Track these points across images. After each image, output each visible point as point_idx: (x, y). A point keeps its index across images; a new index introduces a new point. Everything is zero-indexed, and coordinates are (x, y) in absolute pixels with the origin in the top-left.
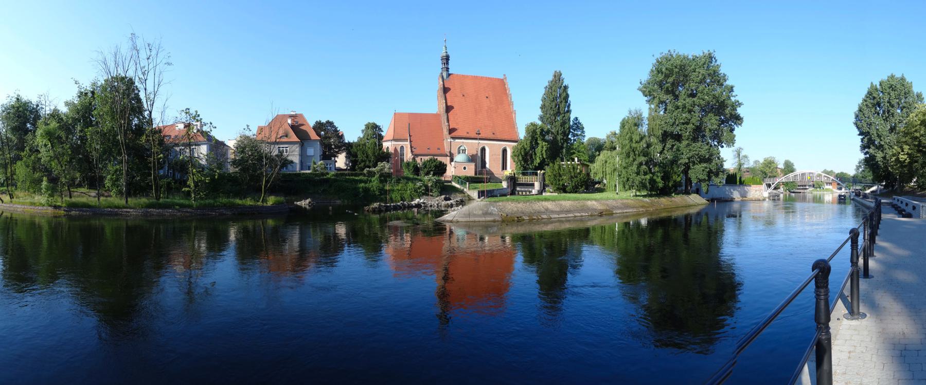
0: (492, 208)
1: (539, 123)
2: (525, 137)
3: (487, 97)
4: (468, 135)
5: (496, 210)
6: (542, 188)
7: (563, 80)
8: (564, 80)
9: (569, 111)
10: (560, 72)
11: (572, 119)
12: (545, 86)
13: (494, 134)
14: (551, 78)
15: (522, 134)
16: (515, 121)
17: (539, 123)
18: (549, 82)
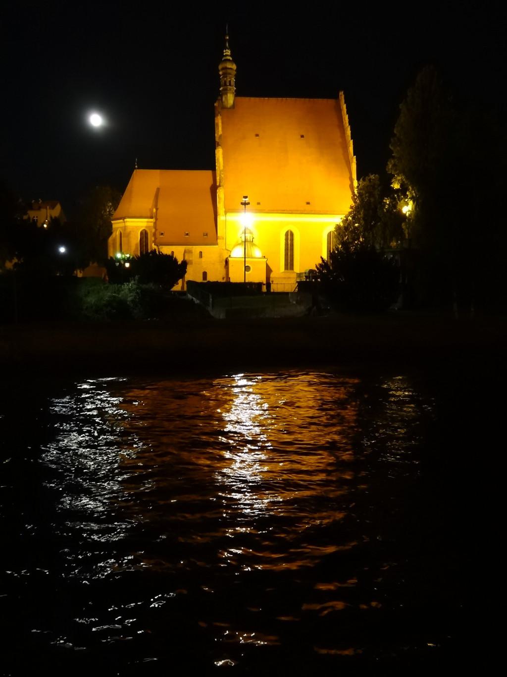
13: (308, 203)
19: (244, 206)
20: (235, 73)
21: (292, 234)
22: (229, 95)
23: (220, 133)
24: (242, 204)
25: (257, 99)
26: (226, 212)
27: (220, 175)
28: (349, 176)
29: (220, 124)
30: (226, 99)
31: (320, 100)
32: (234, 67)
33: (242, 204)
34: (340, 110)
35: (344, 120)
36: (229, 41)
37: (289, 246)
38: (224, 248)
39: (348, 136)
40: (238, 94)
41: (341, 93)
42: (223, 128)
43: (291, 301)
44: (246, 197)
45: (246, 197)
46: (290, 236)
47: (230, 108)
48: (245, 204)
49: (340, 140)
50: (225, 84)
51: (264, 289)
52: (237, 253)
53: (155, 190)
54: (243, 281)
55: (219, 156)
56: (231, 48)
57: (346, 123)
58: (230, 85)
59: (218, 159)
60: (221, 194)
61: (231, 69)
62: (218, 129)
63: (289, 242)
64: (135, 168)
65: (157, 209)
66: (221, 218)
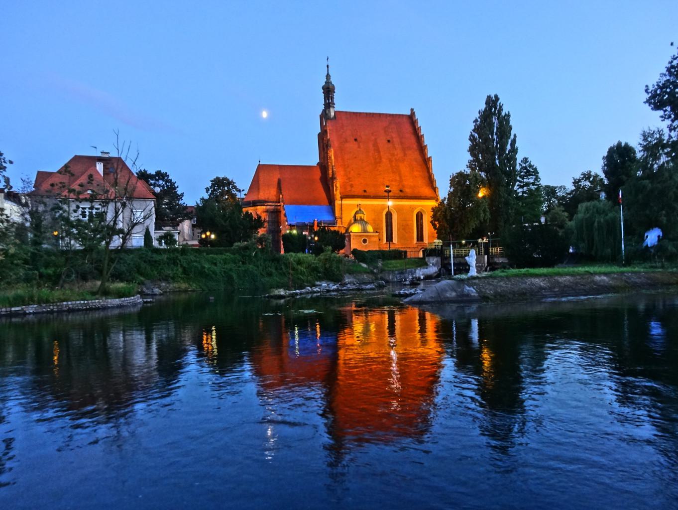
0: (468, 288)
1: (468, 171)
2: (450, 194)
3: (389, 141)
4: (365, 194)
5: (474, 291)
6: (486, 265)
7: (501, 107)
8: (503, 107)
9: (514, 150)
10: (496, 96)
11: (518, 161)
12: (475, 119)
13: (401, 191)
14: (483, 107)
15: (444, 190)
16: (432, 172)
17: (468, 171)
18: (479, 112)
19: (387, 193)
21: (391, 215)
22: (331, 109)
23: (328, 138)
26: (342, 198)
27: (332, 169)
29: (328, 131)
30: (329, 111)
33: (386, 191)
38: (341, 225)
42: (330, 134)
43: (428, 263)
44: (387, 186)
46: (389, 216)
48: (389, 191)
51: (403, 253)
52: (356, 229)
53: (276, 180)
55: (331, 155)
59: (330, 157)
60: (338, 184)
62: (327, 134)
65: (283, 196)
66: (338, 202)
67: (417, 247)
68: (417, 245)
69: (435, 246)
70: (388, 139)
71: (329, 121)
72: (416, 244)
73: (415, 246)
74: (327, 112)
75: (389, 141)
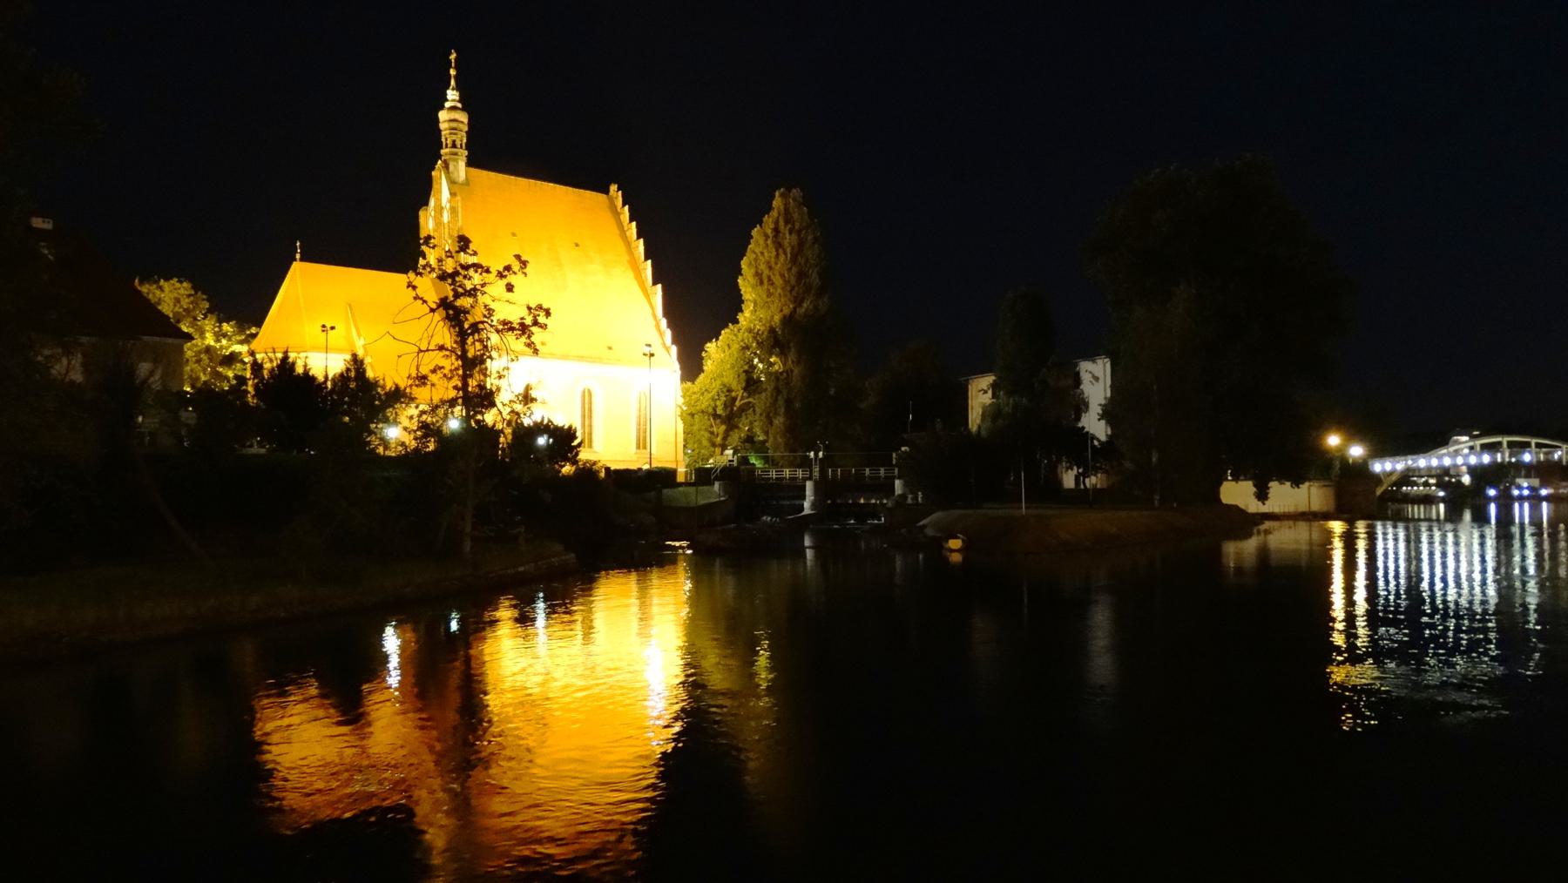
13: (610, 348)
19: (647, 358)
20: (466, 129)
23: (460, 223)
24: (645, 355)
25: (501, 176)
28: (651, 311)
29: (460, 210)
30: (456, 167)
31: (588, 193)
32: (466, 120)
33: (645, 355)
34: (617, 215)
35: (626, 229)
36: (456, 77)
37: (586, 411)
39: (640, 253)
40: (471, 163)
41: (613, 188)
44: (649, 345)
45: (649, 345)
47: (462, 184)
48: (652, 355)
49: (626, 258)
50: (454, 146)
54: (646, 467)
56: (458, 88)
57: (632, 233)
58: (461, 147)
61: (462, 122)
63: (587, 406)
64: (295, 260)
67: (637, 461)
68: (638, 456)
69: (730, 461)
70: (576, 241)
71: (456, 188)
72: (636, 453)
73: (635, 458)
74: (451, 167)
75: (577, 245)
